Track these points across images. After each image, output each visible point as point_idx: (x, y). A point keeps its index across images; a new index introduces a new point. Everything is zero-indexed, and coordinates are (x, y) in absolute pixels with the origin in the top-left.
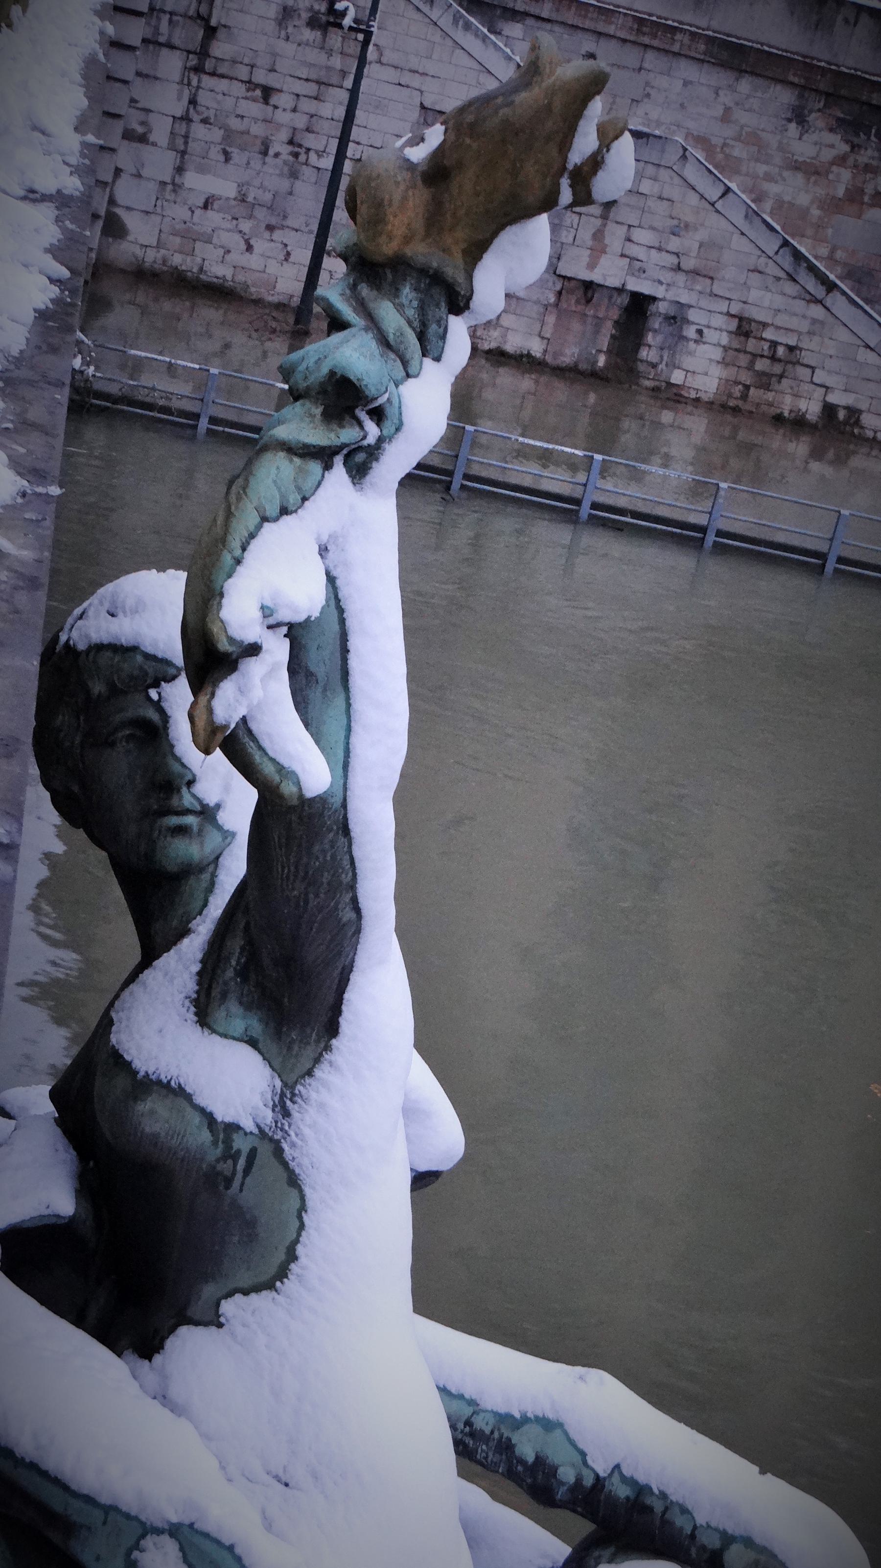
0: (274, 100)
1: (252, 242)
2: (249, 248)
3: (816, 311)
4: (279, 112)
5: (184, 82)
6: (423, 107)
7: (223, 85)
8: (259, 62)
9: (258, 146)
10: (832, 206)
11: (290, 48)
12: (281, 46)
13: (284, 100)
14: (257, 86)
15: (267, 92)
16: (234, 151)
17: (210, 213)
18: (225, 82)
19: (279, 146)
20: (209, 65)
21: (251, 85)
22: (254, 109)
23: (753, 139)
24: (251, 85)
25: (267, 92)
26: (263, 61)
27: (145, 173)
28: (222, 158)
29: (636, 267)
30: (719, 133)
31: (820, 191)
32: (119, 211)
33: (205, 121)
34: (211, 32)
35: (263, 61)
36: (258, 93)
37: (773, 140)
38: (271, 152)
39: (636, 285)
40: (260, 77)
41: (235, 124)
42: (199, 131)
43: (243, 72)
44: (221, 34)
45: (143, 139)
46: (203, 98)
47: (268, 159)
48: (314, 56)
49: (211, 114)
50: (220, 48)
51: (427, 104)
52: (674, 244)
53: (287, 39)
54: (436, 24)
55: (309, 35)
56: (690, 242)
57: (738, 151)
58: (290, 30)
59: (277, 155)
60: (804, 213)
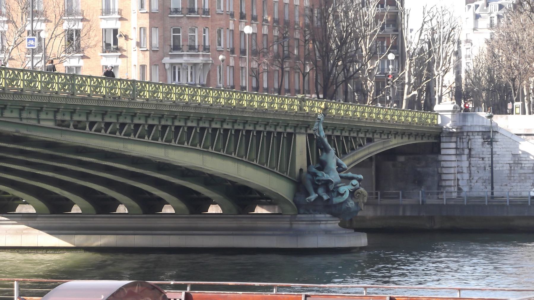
0: (485, 159)
1: (487, 187)
2: (486, 188)
4: (486, 161)
5: (468, 160)
6: (512, 154)
7: (474, 159)
8: (480, 153)
9: (483, 169)
11: (485, 150)
12: (483, 149)
14: (481, 158)
15: (483, 159)
16: (480, 172)
17: (477, 183)
18: (475, 158)
20: (471, 156)
21: (480, 158)
22: (481, 162)
24: (480, 158)
26: (481, 153)
27: (464, 179)
28: (477, 172)
32: (461, 187)
33: (473, 166)
34: (470, 150)
35: (481, 153)
36: (481, 159)
38: (486, 169)
40: (481, 156)
41: (478, 165)
42: (472, 169)
43: (477, 156)
44: (472, 150)
45: (462, 172)
46: (472, 162)
47: (486, 171)
49: (473, 165)
50: (473, 153)
51: (513, 153)
53: (484, 148)
54: (510, 138)
58: (484, 146)
59: (487, 170)
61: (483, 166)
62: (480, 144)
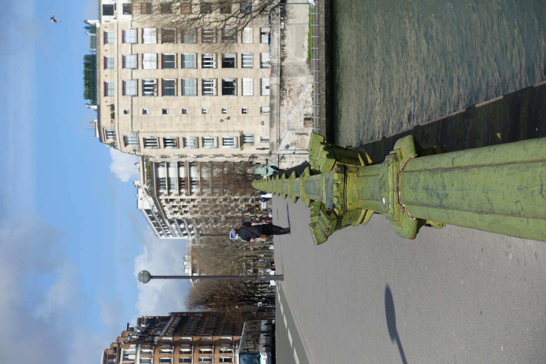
3: (301, 100)
10: (291, 99)
11: (288, 161)
13: (293, 160)
19: (298, 160)
23: (286, 109)
25: (293, 162)
29: (301, 120)
30: (287, 113)
31: (290, 101)
37: (286, 107)
39: (303, 120)
40: (291, 163)
48: (288, 158)
52: (298, 117)
55: (286, 159)
56: (297, 116)
57: (288, 110)
60: (293, 102)
61: (297, 162)
62: (285, 164)
